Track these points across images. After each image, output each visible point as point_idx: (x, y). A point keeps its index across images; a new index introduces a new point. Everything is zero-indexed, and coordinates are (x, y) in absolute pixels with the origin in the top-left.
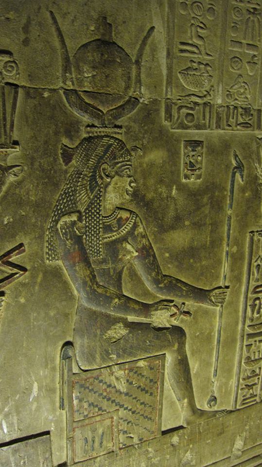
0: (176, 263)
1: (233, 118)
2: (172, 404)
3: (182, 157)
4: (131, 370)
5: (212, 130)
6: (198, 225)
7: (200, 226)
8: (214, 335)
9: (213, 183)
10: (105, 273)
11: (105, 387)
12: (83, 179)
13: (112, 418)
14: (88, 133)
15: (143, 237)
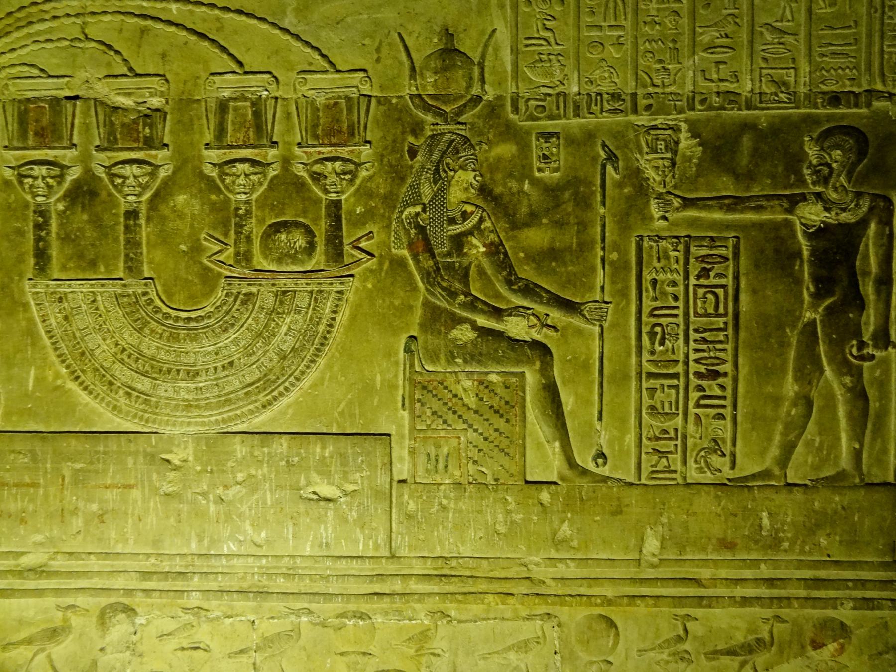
0: (533, 265)
1: (596, 105)
2: (539, 446)
3: (534, 150)
4: (481, 383)
5: (568, 119)
6: (560, 224)
7: (563, 225)
8: (594, 363)
9: (576, 177)
10: (450, 267)
11: (450, 396)
12: (427, 172)
13: (459, 437)
14: (432, 130)
15: (492, 232)
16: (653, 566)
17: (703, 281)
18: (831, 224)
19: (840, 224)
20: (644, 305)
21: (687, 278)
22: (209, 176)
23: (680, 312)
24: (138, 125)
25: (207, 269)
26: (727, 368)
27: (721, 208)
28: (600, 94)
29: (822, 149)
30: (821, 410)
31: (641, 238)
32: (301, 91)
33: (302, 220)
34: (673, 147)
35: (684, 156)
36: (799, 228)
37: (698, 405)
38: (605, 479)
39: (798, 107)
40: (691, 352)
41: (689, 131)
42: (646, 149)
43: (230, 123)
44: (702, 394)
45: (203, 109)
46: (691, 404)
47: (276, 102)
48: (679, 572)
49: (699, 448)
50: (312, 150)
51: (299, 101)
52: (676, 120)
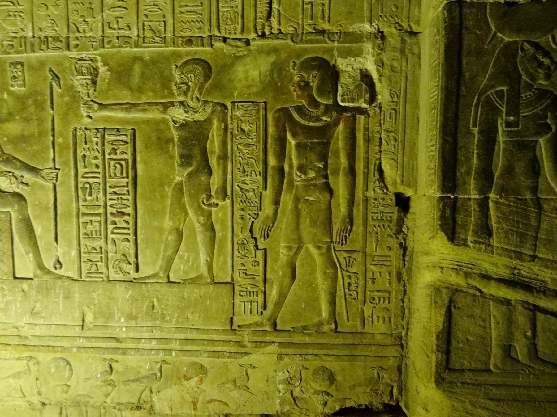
9: (35, 91)
16: (90, 329)
17: (113, 157)
18: (189, 121)
19: (195, 121)
20: (79, 171)
21: (104, 154)
23: (100, 176)
26: (129, 210)
27: (122, 110)
28: (47, 38)
29: (182, 73)
30: (187, 237)
31: (76, 129)
34: (95, 73)
35: (102, 77)
36: (172, 124)
37: (112, 233)
38: (61, 277)
39: (167, 47)
40: (108, 200)
41: (102, 61)
42: (76, 73)
44: (115, 226)
46: (109, 232)
48: (107, 333)
49: (115, 259)
52: (94, 54)
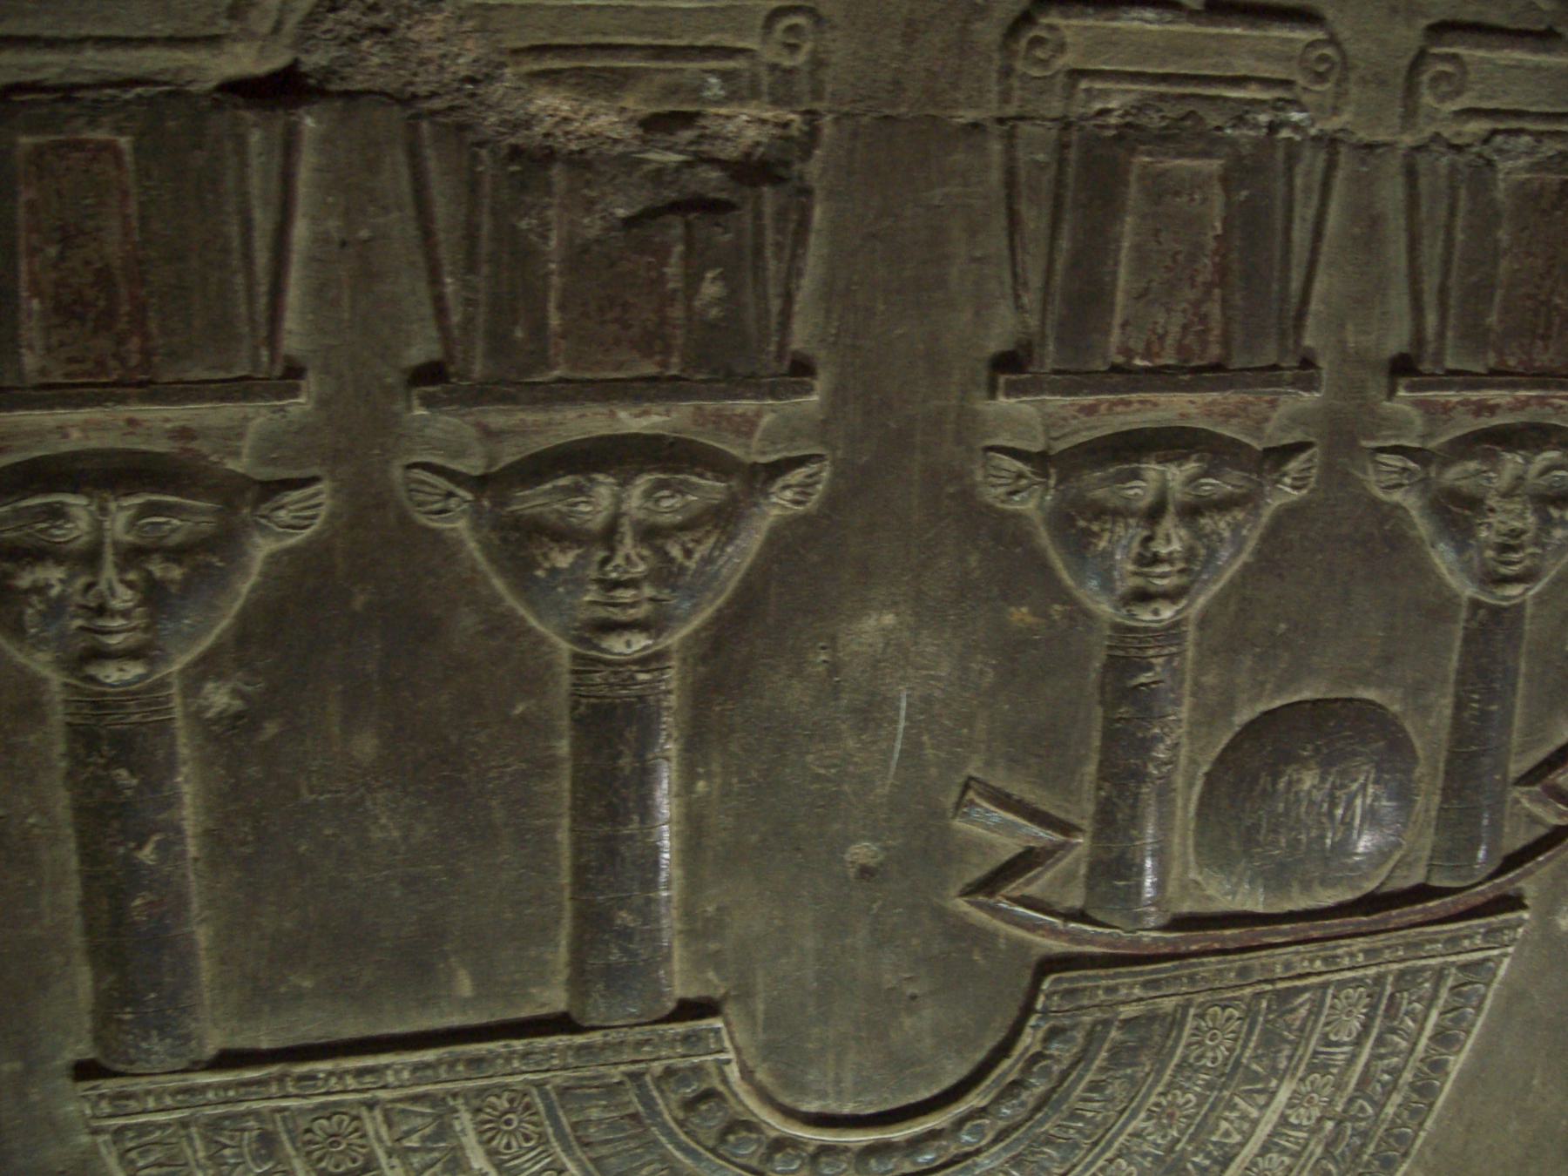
22: (1004, 516)
24: (663, 252)
25: (964, 932)
32: (1432, 117)
33: (1370, 694)
43: (1124, 256)
45: (995, 177)
47: (1331, 166)
50: (1452, 396)
51: (1423, 162)
